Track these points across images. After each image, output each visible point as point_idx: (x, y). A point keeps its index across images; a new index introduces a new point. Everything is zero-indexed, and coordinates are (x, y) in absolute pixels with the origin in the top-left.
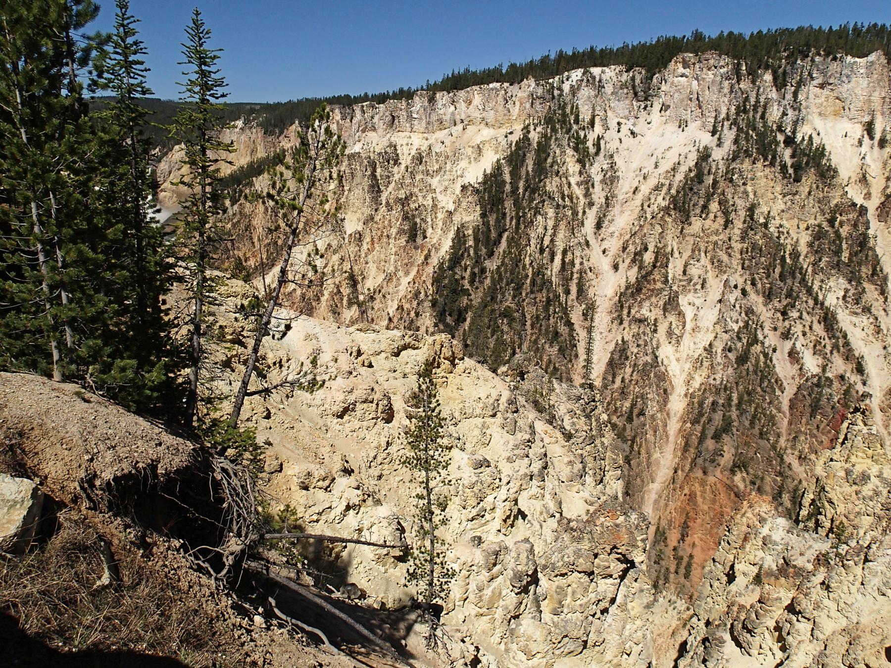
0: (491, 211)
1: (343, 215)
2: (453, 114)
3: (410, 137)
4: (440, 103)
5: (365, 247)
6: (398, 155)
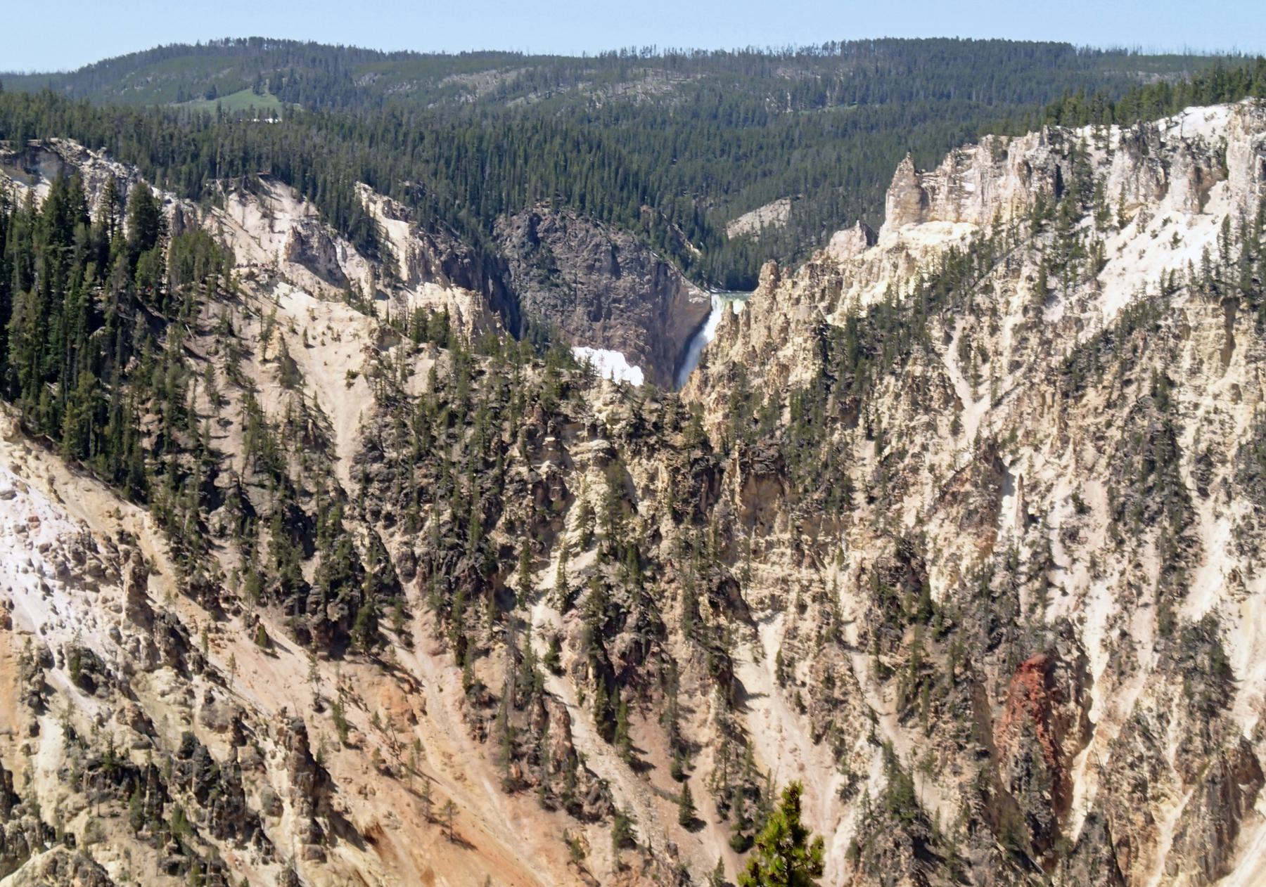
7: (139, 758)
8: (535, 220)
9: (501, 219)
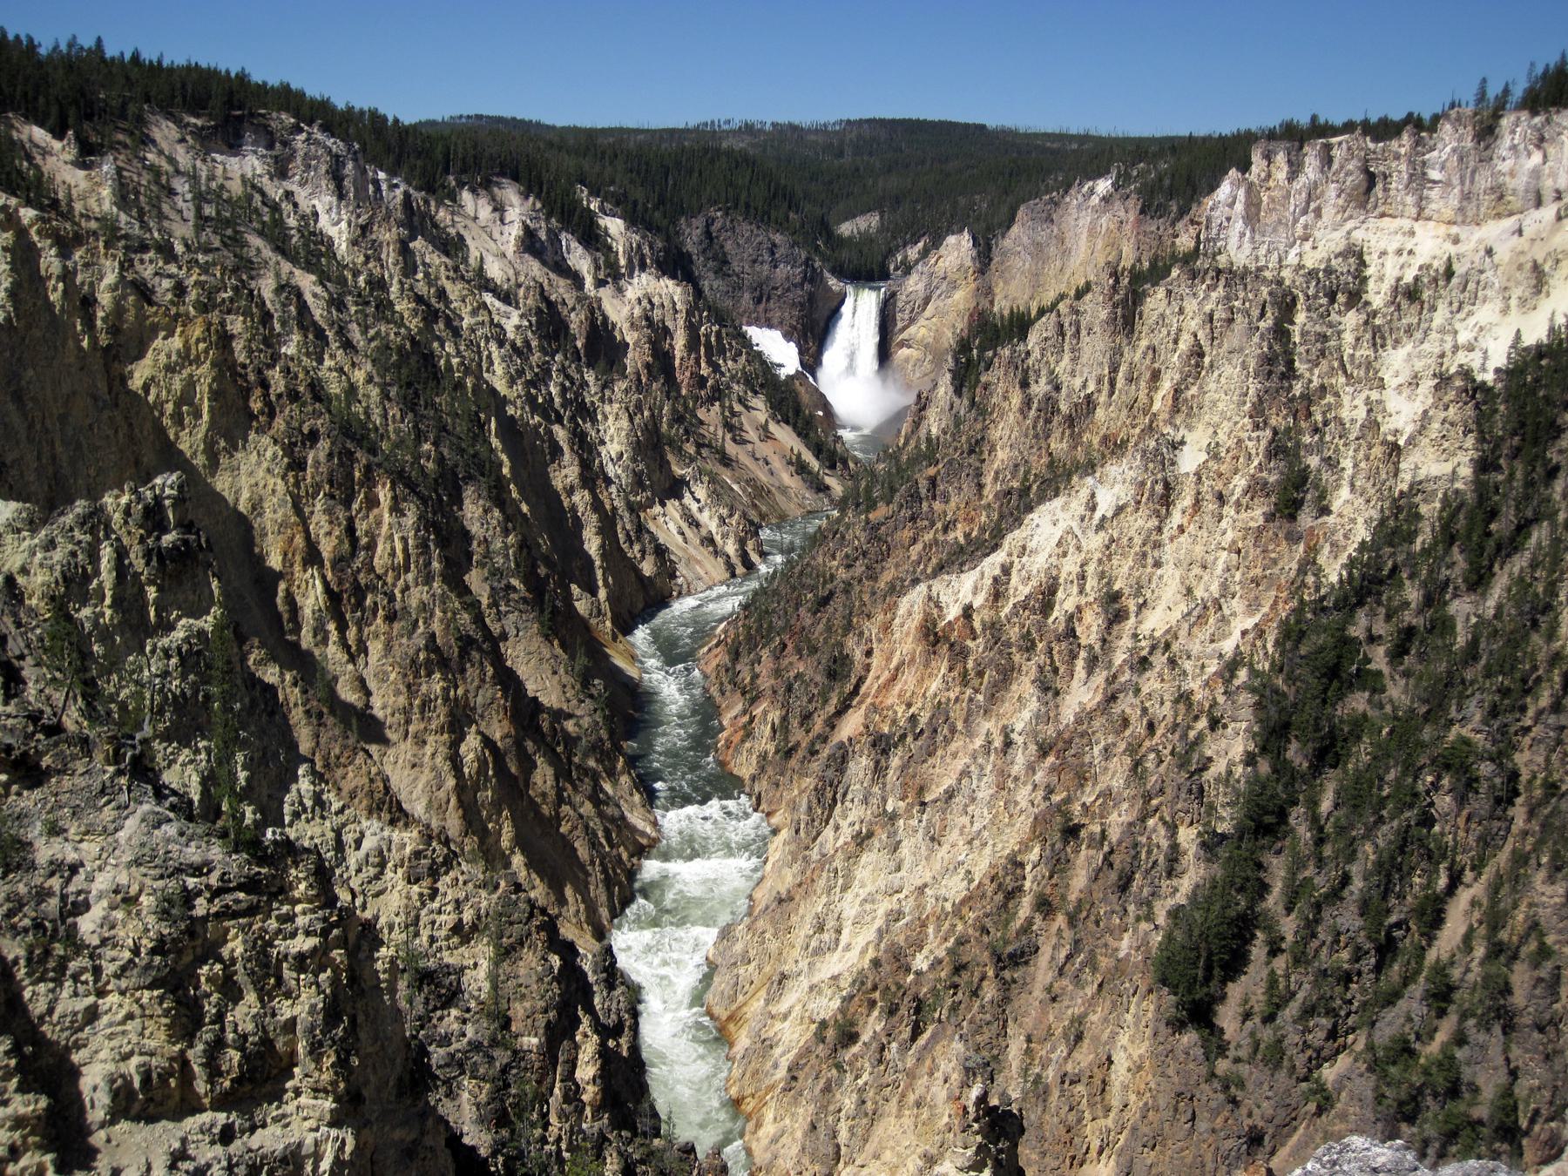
0: (1516, 453)
1: (1183, 431)
2: (1536, 173)
3: (1412, 233)
4: (1506, 142)
5: (1177, 518)
6: (1364, 280)
8: (710, 223)
9: (683, 220)
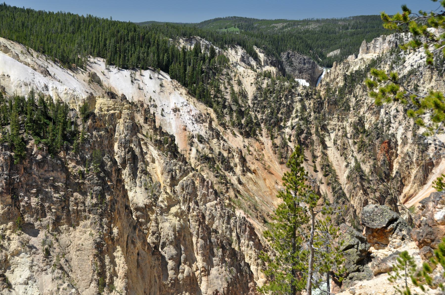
7: (210, 156)
8: (289, 53)
9: (282, 53)
